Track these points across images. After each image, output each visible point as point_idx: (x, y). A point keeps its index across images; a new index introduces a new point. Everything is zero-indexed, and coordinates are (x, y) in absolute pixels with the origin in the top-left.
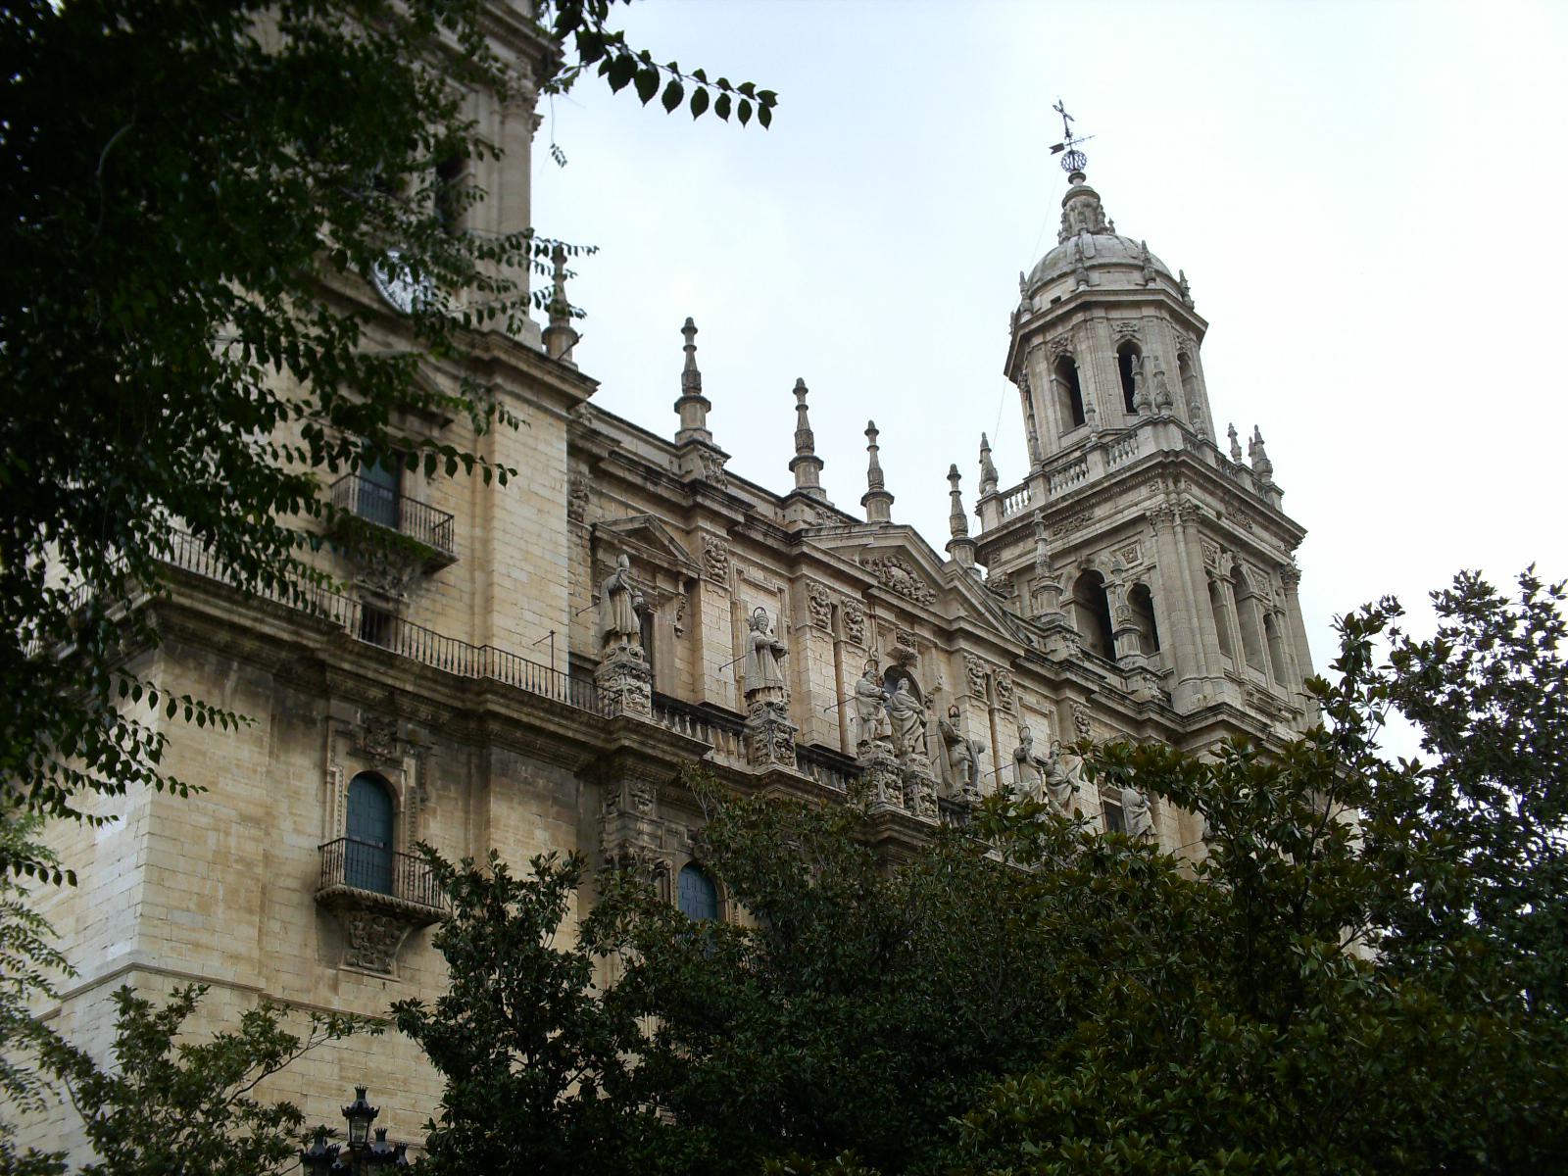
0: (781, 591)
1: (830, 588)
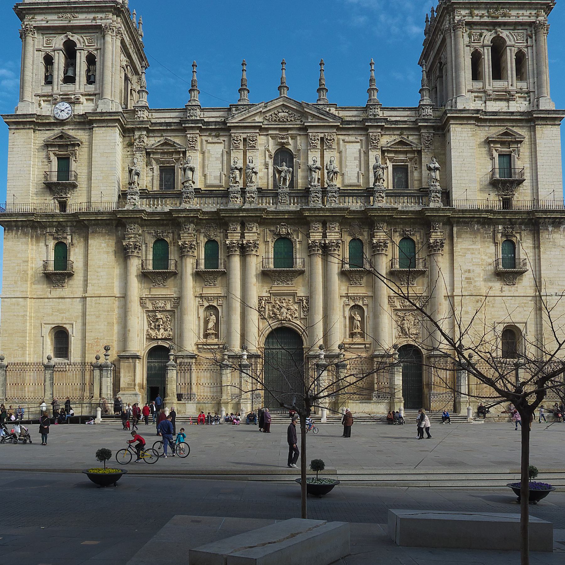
0: (224, 141)
1: (243, 133)
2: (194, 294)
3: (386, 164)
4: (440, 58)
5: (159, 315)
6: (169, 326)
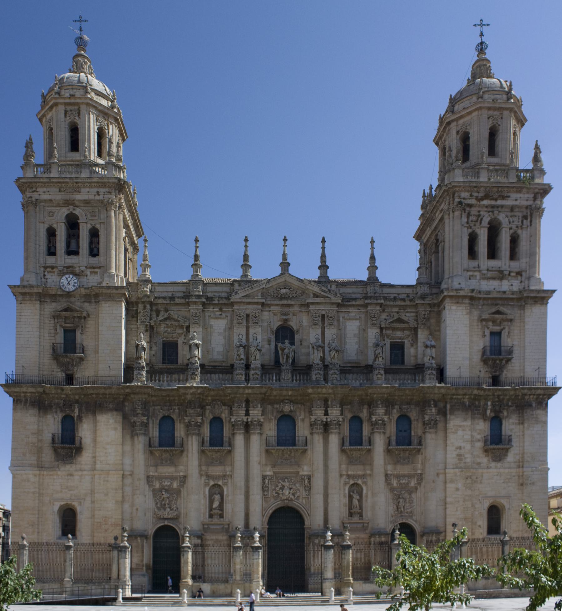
2: (199, 473)
3: (384, 340)
4: (437, 235)
5: (165, 495)
6: (175, 506)
